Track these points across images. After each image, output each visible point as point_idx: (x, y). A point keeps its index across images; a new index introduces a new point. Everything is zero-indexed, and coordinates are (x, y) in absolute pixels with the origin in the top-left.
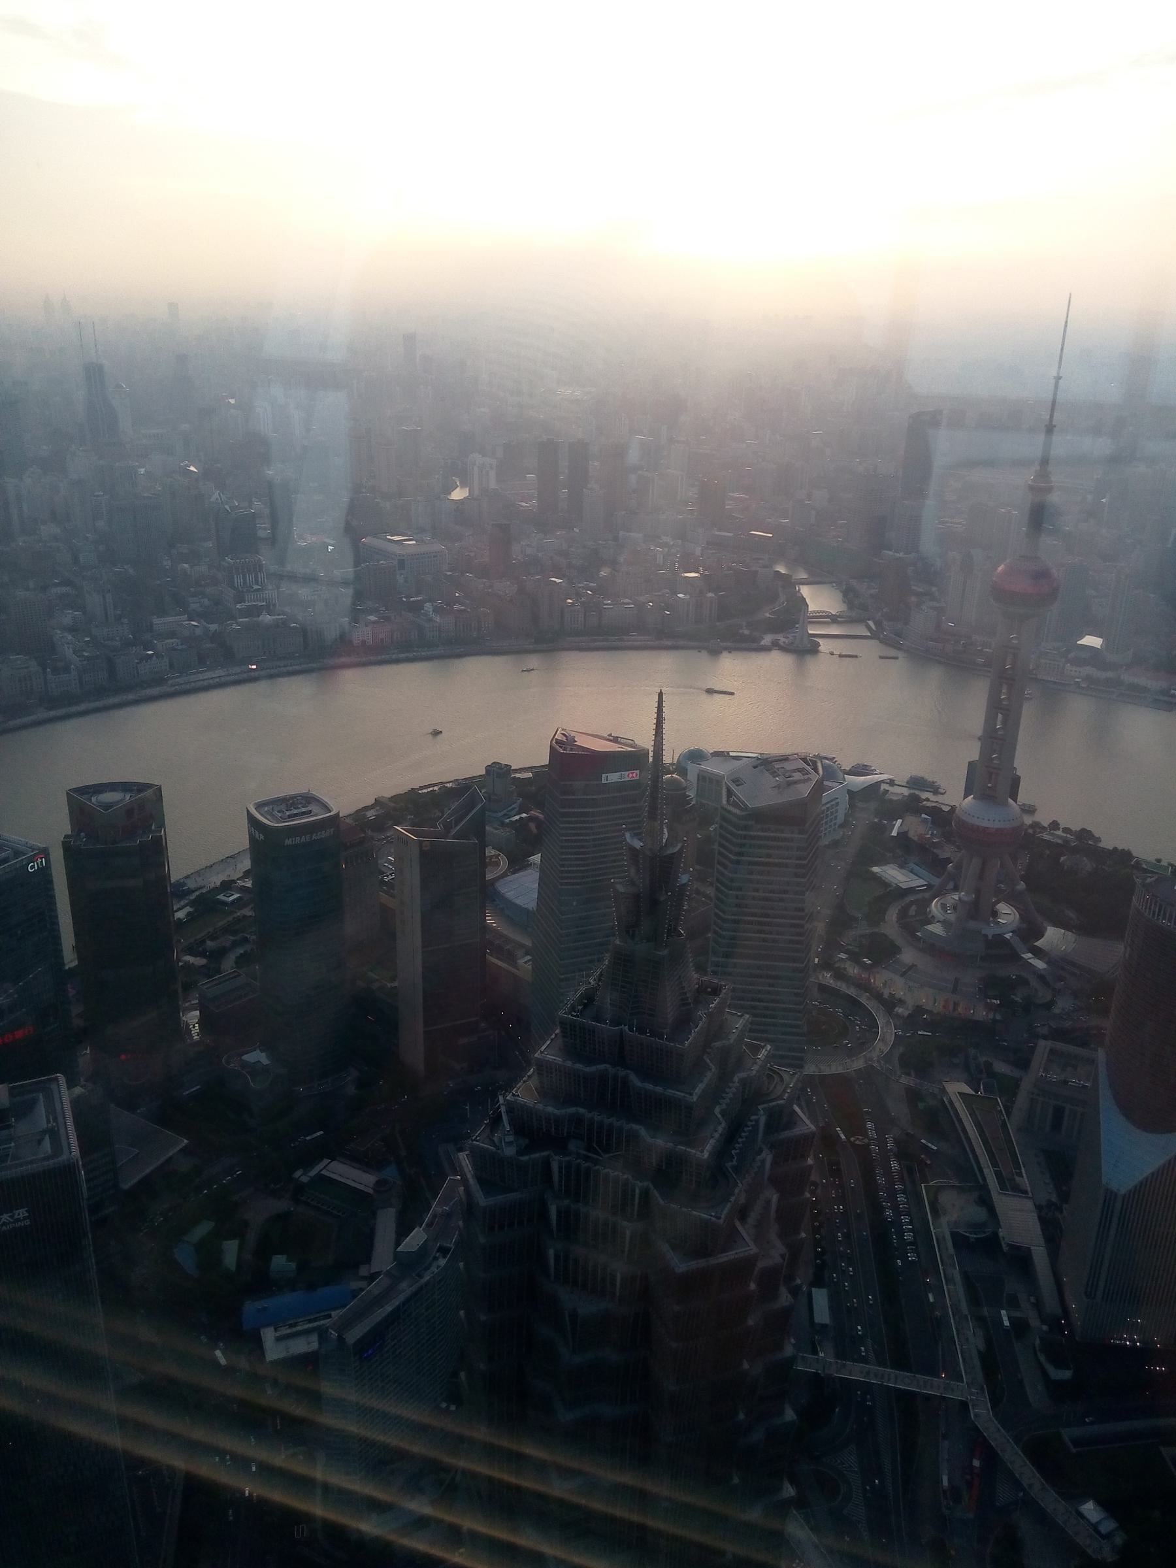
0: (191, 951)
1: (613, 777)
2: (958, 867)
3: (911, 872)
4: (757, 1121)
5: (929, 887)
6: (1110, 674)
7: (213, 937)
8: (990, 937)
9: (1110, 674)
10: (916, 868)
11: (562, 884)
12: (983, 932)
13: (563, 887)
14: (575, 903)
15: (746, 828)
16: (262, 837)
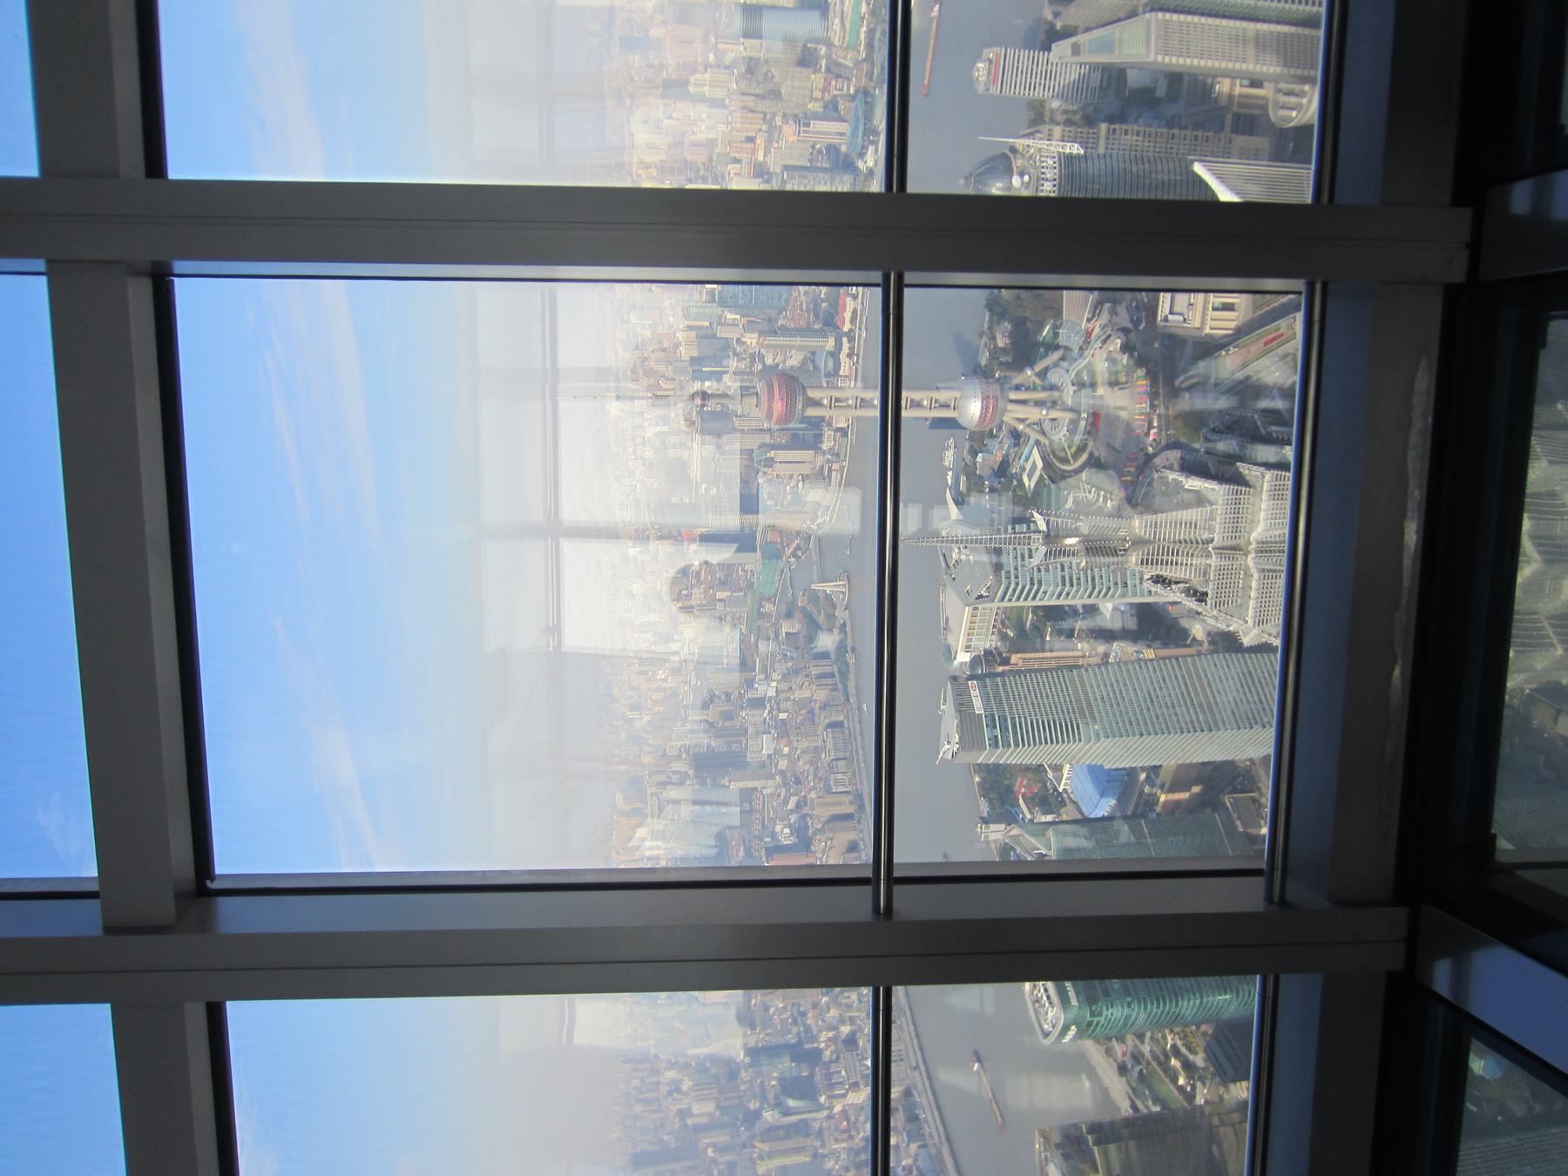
0: (1190, 1097)
1: (978, 706)
2: (1021, 420)
3: (1027, 459)
4: (1277, 432)
5: (1038, 443)
6: (845, 340)
7: (1174, 1080)
8: (1075, 388)
9: (845, 340)
10: (1023, 458)
11: (1080, 740)
12: (1072, 393)
13: (1083, 739)
14: (1097, 727)
15: (1008, 578)
16: (1073, 1027)
